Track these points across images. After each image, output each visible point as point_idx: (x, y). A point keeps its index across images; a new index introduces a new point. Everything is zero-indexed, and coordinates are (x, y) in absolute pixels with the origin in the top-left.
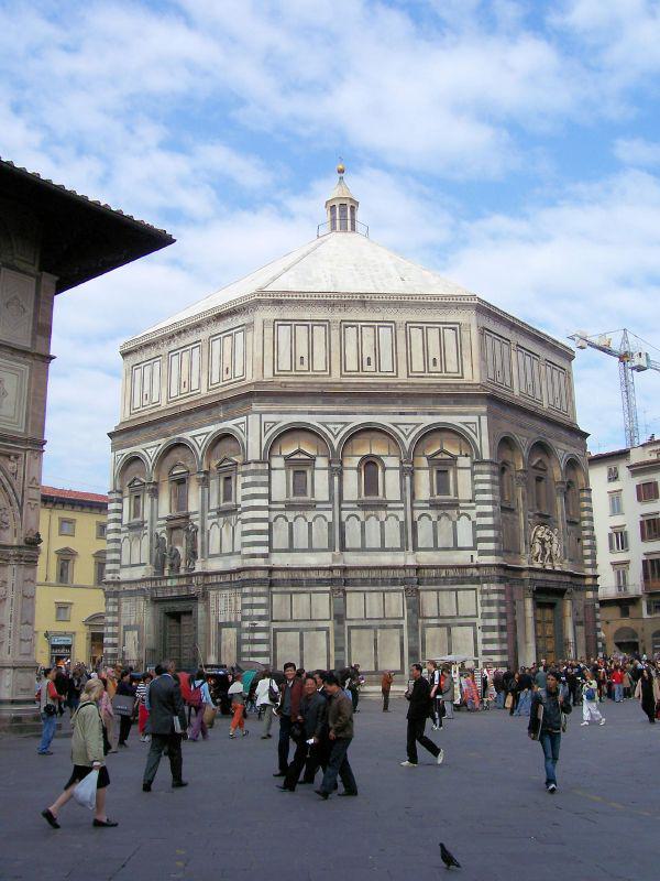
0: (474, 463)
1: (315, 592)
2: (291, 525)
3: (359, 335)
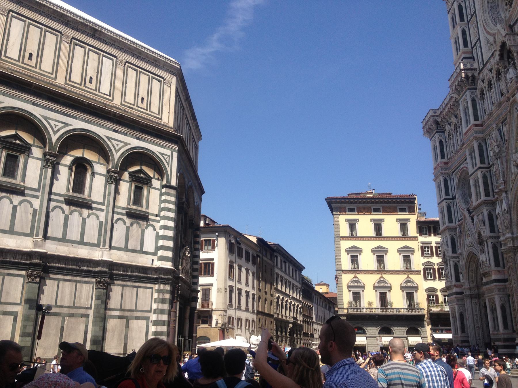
0: (163, 187)
1: (9, 275)
3: (86, 56)
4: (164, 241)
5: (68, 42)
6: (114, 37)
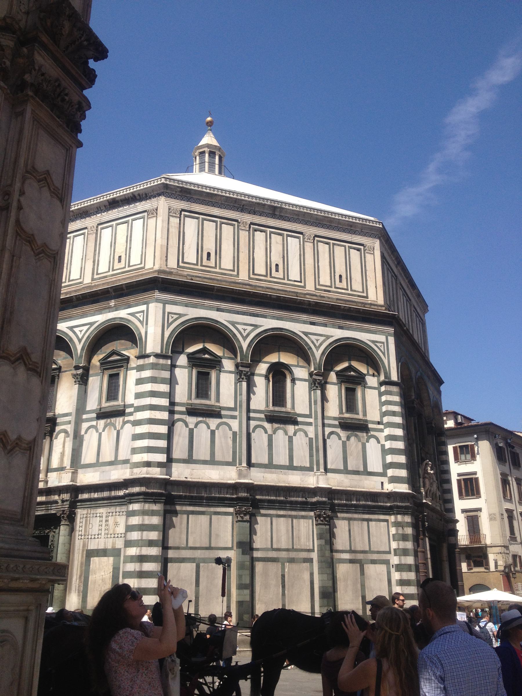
0: (381, 384)
2: (191, 432)
4: (393, 455)
5: (246, 230)
6: (297, 211)
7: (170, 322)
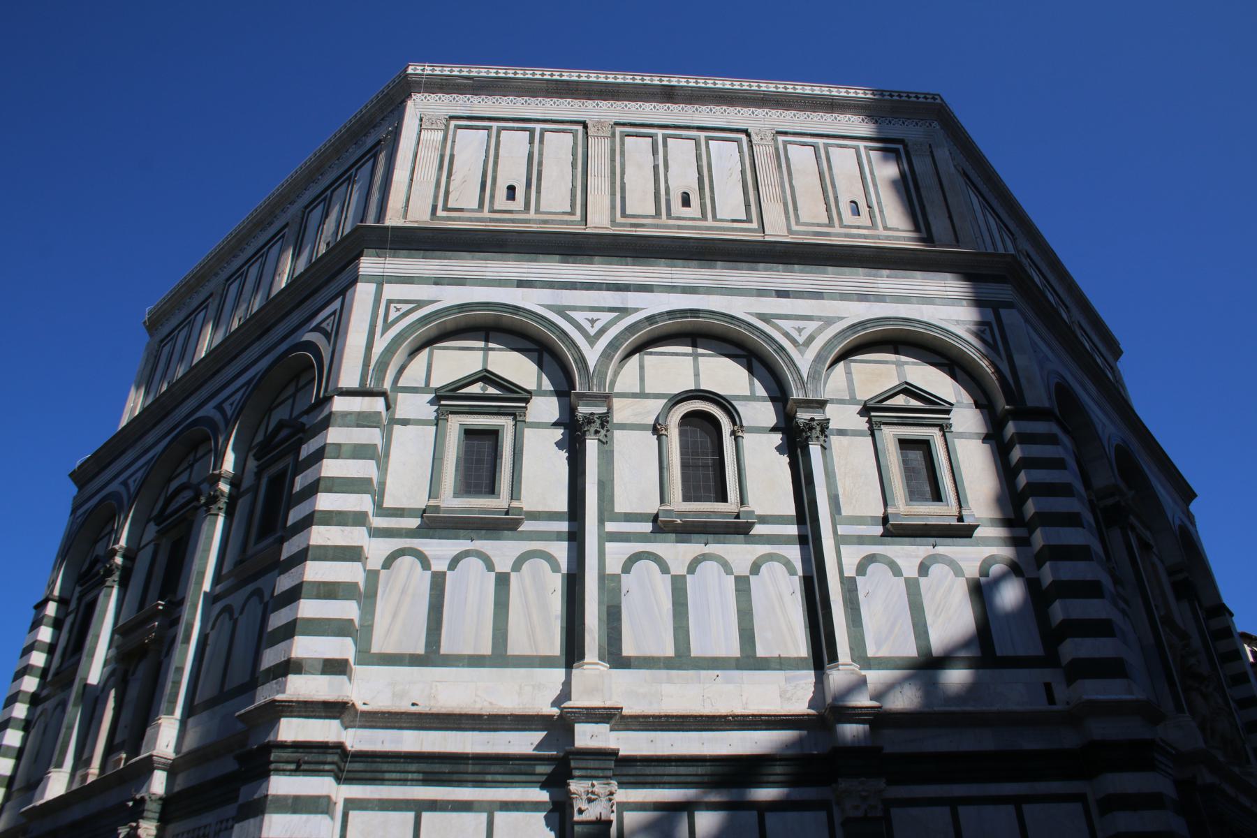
2: (438, 583)
7: (390, 319)
